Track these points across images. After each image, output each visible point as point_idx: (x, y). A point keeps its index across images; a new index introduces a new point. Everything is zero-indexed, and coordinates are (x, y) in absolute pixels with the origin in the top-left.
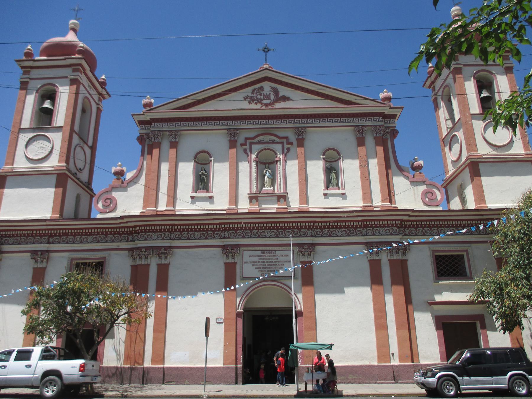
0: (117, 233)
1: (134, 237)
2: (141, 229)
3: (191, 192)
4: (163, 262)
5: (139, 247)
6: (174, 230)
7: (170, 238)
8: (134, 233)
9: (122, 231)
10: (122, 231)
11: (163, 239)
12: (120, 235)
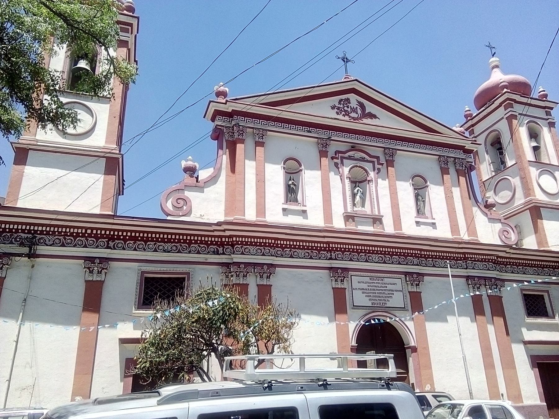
0: (204, 242)
1: (226, 249)
2: (238, 240)
3: (283, 204)
4: (265, 282)
5: (234, 262)
6: (275, 245)
7: (271, 254)
8: (226, 245)
9: (211, 241)
10: (211, 241)
11: (263, 255)
12: (208, 245)
